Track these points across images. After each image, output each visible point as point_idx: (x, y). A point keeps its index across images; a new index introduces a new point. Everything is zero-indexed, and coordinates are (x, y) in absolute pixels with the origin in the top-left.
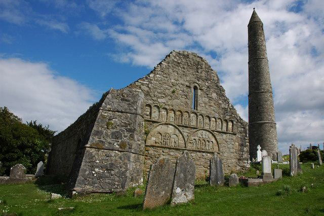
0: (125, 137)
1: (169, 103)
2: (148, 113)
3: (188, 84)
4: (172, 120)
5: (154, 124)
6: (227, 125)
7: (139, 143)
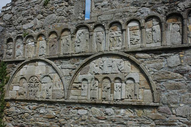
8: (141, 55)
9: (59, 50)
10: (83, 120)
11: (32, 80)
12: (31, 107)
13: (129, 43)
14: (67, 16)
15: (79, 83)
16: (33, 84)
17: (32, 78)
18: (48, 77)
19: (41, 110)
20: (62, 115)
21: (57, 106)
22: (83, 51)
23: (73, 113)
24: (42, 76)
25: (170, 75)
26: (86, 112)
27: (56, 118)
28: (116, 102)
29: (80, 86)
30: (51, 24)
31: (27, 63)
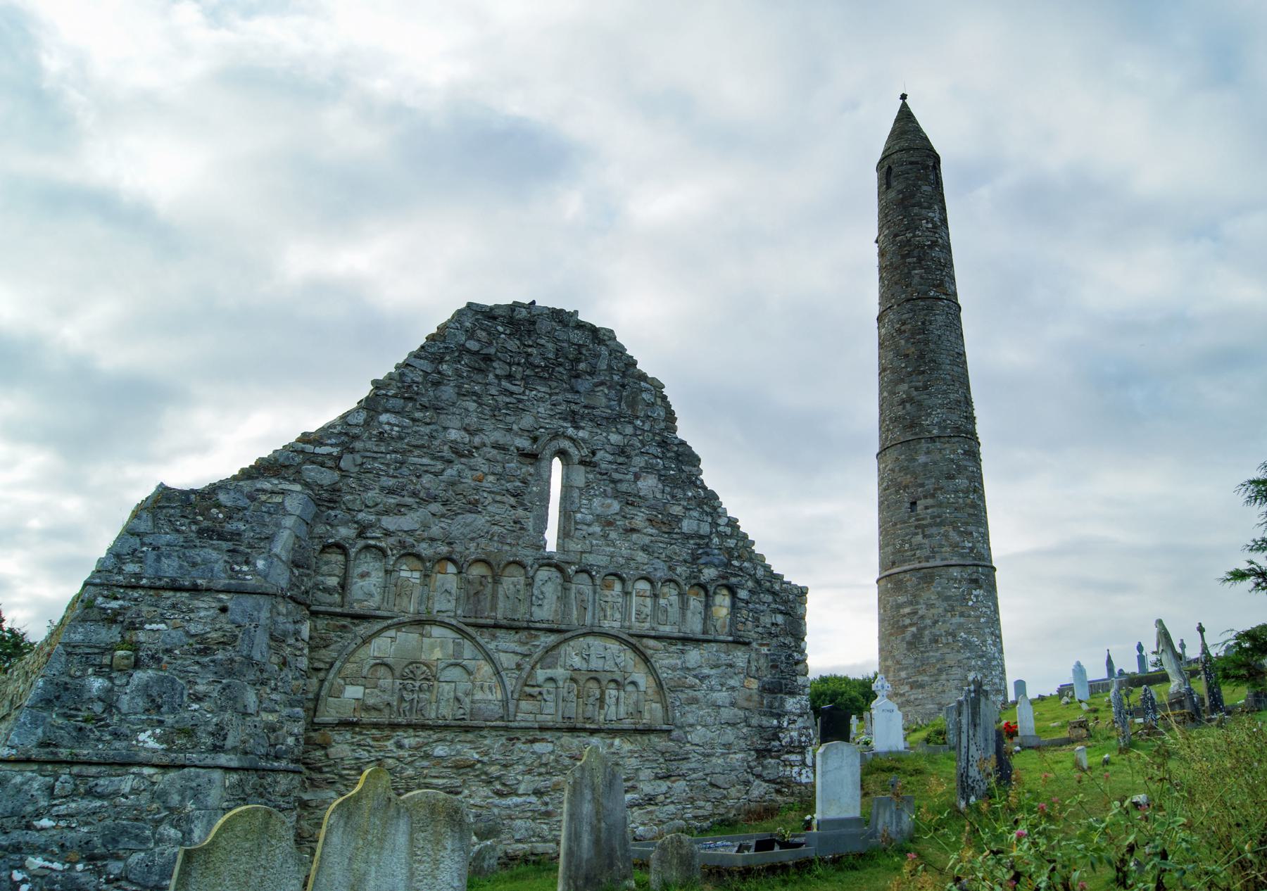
0: (198, 698)
1: (435, 530)
2: (333, 581)
3: (524, 443)
4: (443, 605)
5: (363, 629)
6: (708, 606)
7: (272, 718)
8: (651, 643)
9: (494, 607)
10: (541, 765)
11: (412, 672)
12: (406, 742)
13: (633, 619)
15: (539, 686)
17: (410, 667)
19: (436, 750)
20: (495, 757)
21: (481, 736)
23: (522, 751)
24: (443, 665)
25: (687, 680)
26: (550, 747)
28: (609, 726)
29: (540, 693)
30: (472, 539)
31: (399, 626)
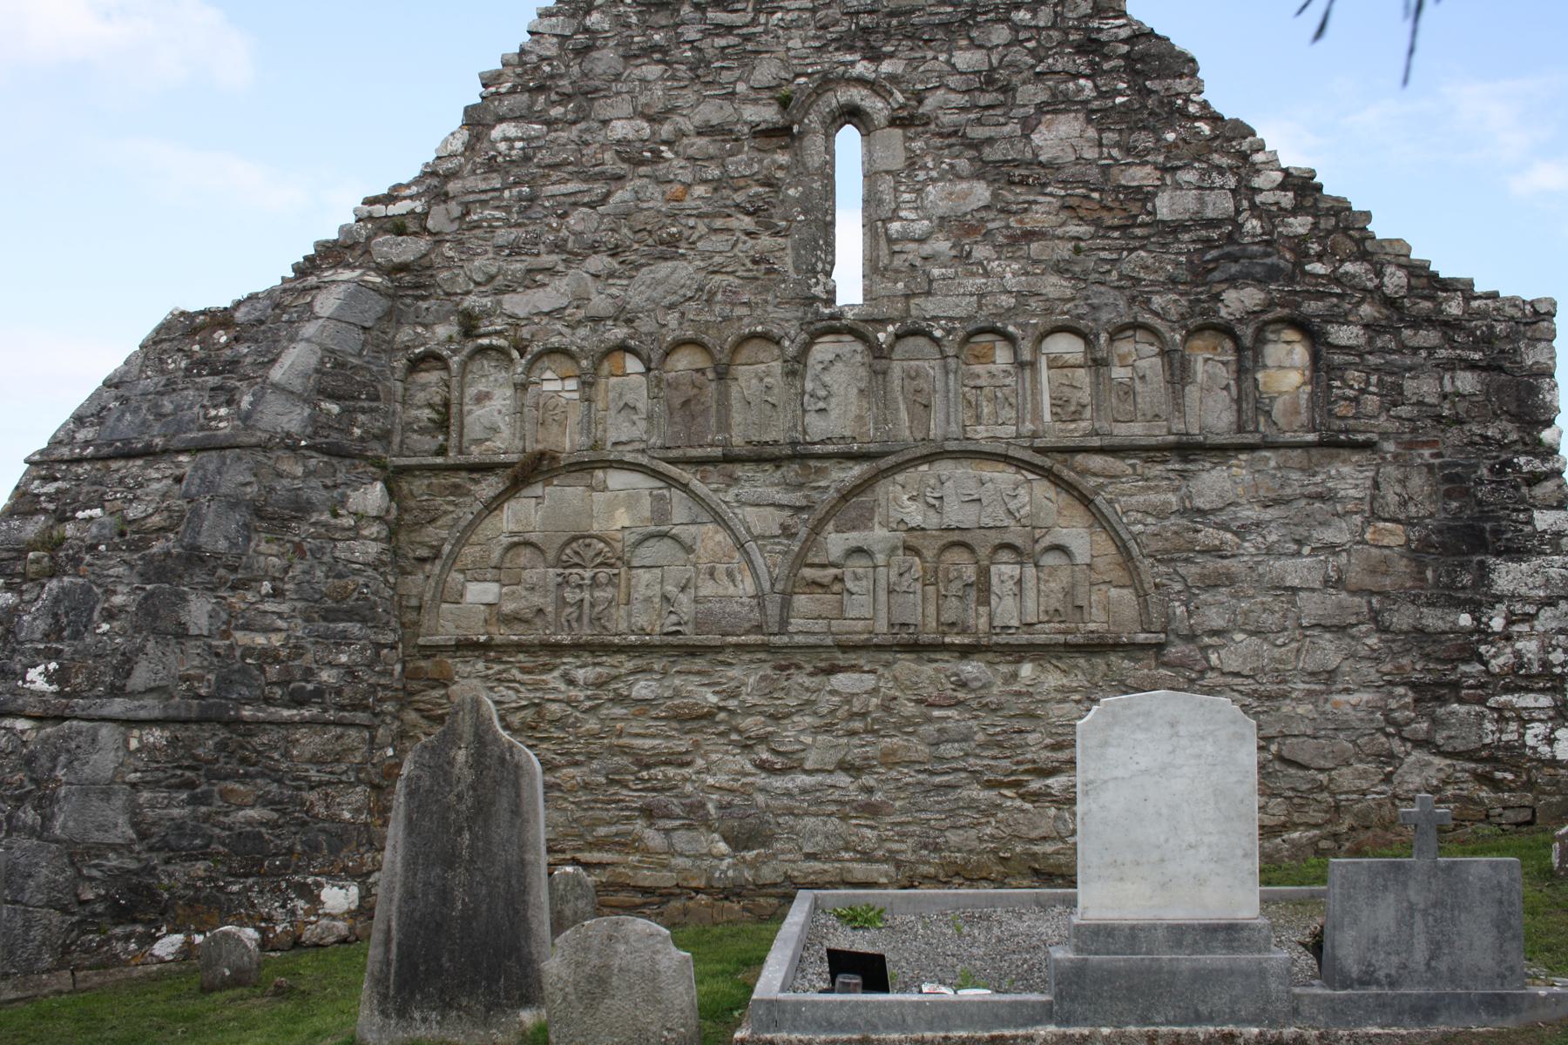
9: (724, 425)
14: (756, 278)
16: (588, 574)
17: (574, 545)
18: (668, 541)
21: (722, 663)
22: (847, 433)
24: (633, 538)
27: (722, 716)
29: (838, 579)
30: (671, 306)
